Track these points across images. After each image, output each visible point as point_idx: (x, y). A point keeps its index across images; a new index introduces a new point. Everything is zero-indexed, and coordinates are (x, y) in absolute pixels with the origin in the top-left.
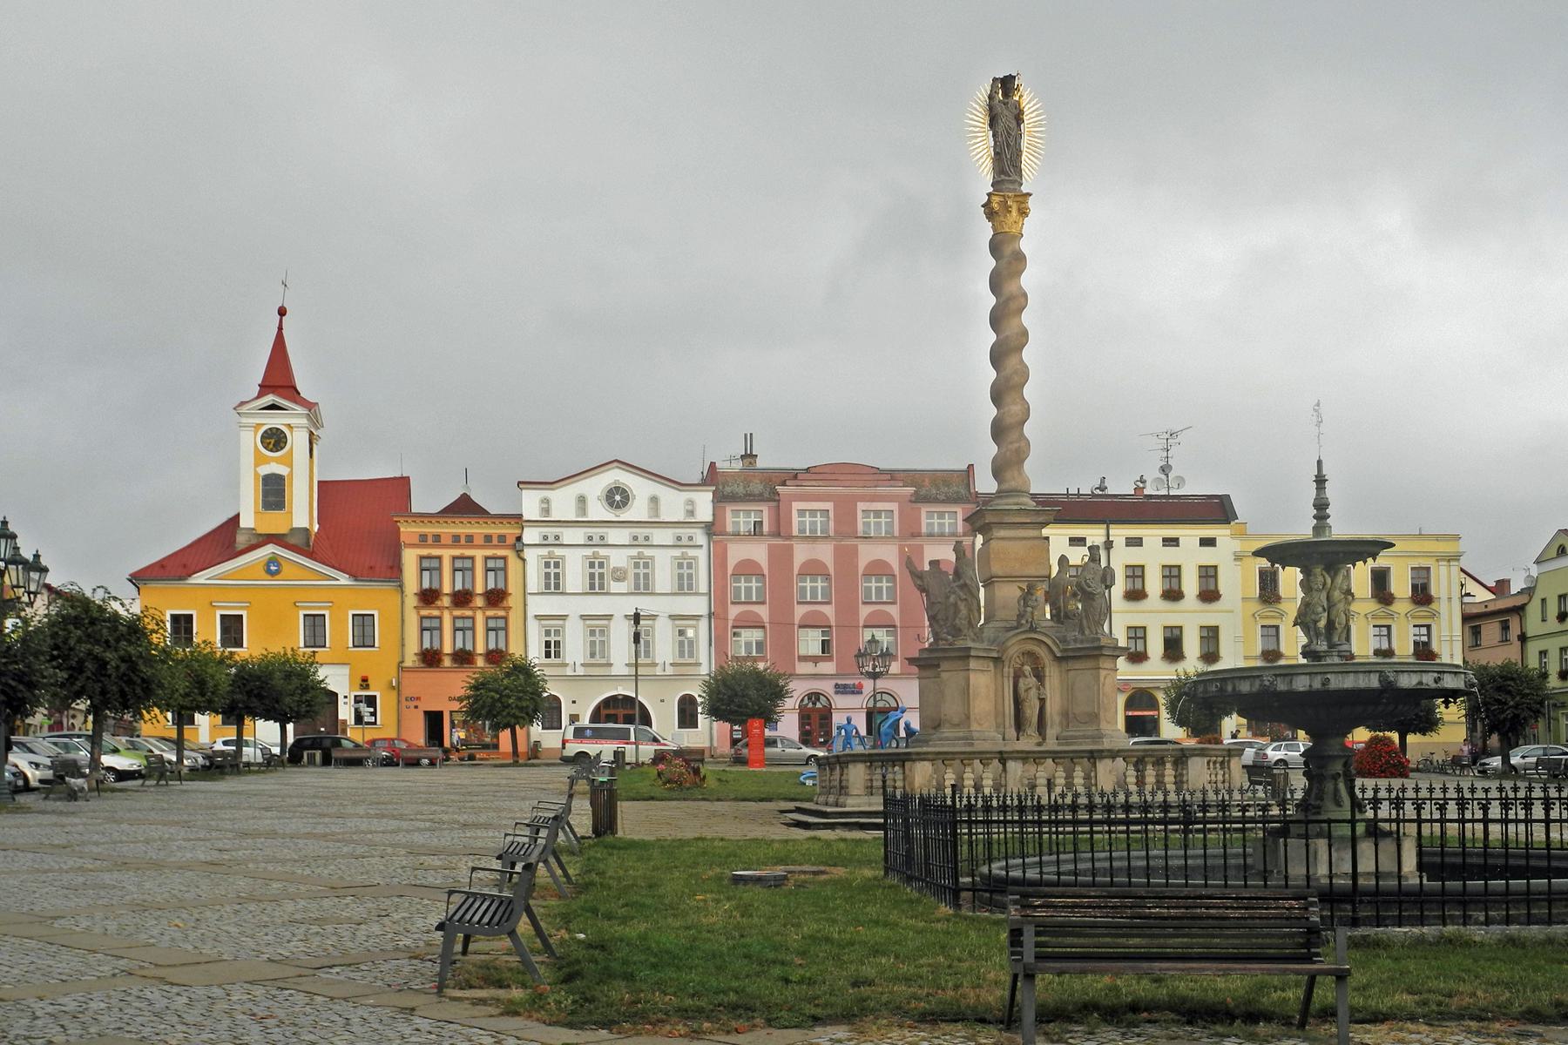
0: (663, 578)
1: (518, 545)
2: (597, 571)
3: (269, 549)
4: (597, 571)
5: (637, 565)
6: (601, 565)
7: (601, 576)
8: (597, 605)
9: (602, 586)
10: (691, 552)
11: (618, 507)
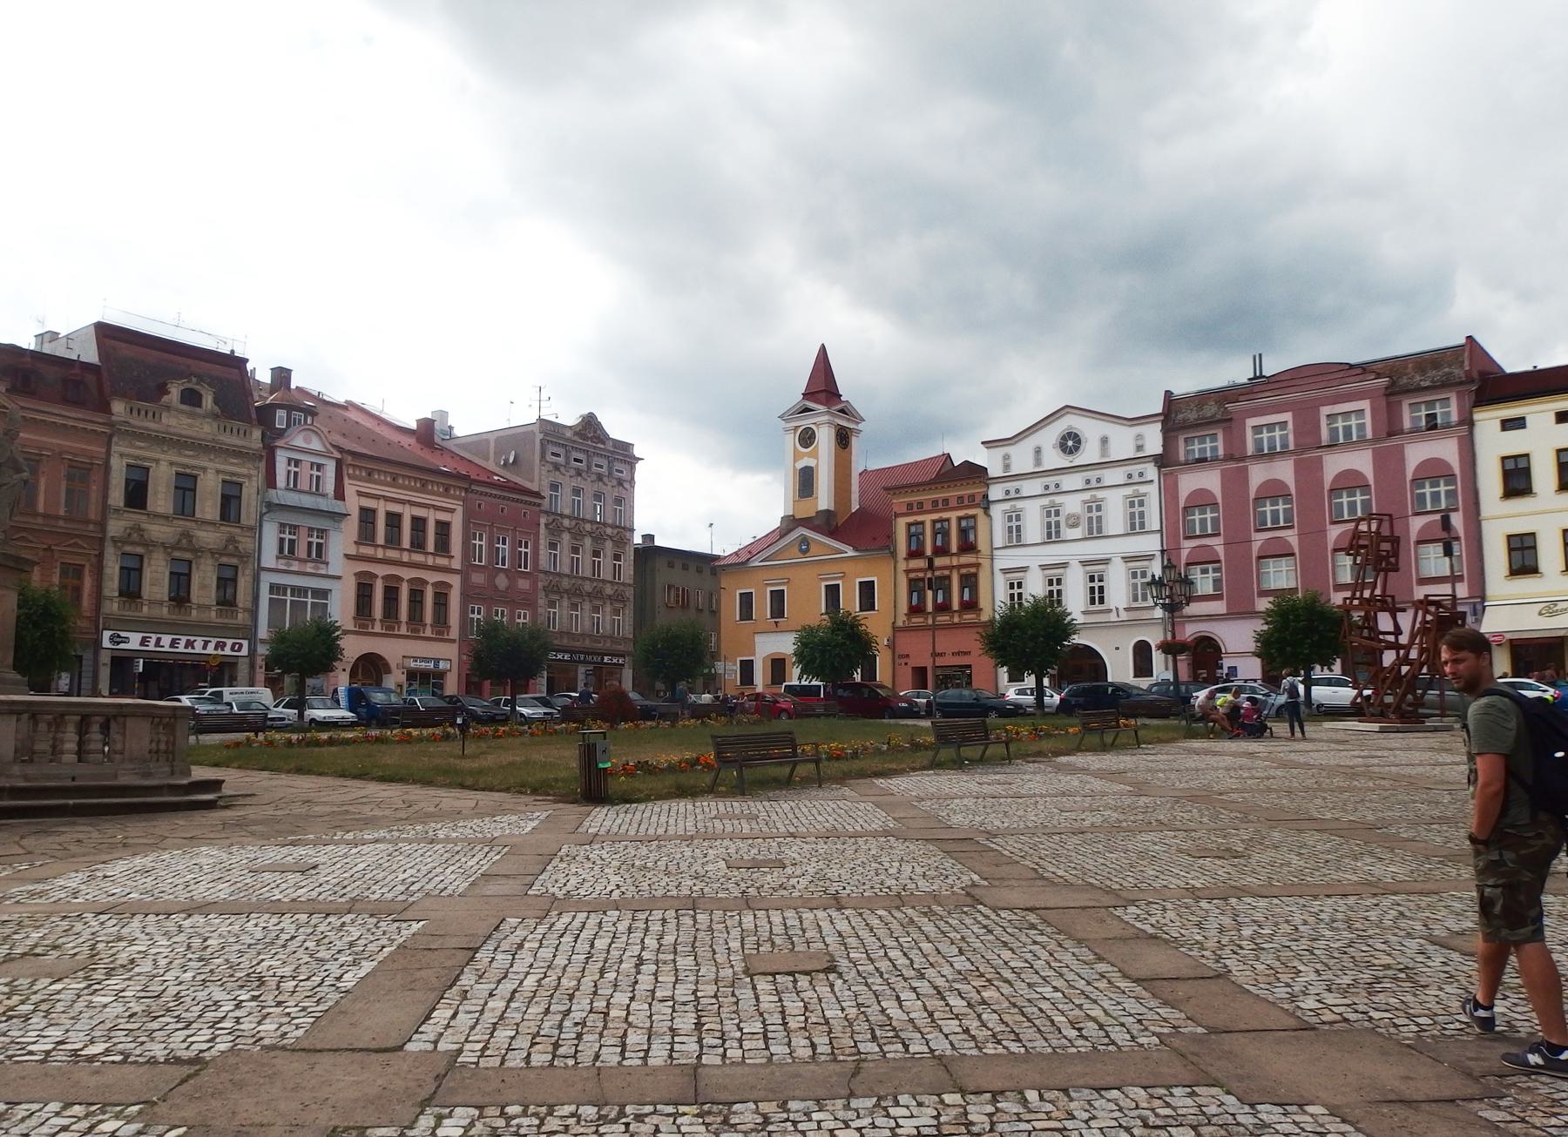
0: (1115, 518)
1: (986, 504)
2: (1053, 519)
3: (802, 531)
4: (1053, 519)
5: (1090, 509)
6: (1057, 513)
7: (1058, 524)
8: (1054, 553)
9: (1058, 533)
10: (1143, 489)
11: (1071, 452)
